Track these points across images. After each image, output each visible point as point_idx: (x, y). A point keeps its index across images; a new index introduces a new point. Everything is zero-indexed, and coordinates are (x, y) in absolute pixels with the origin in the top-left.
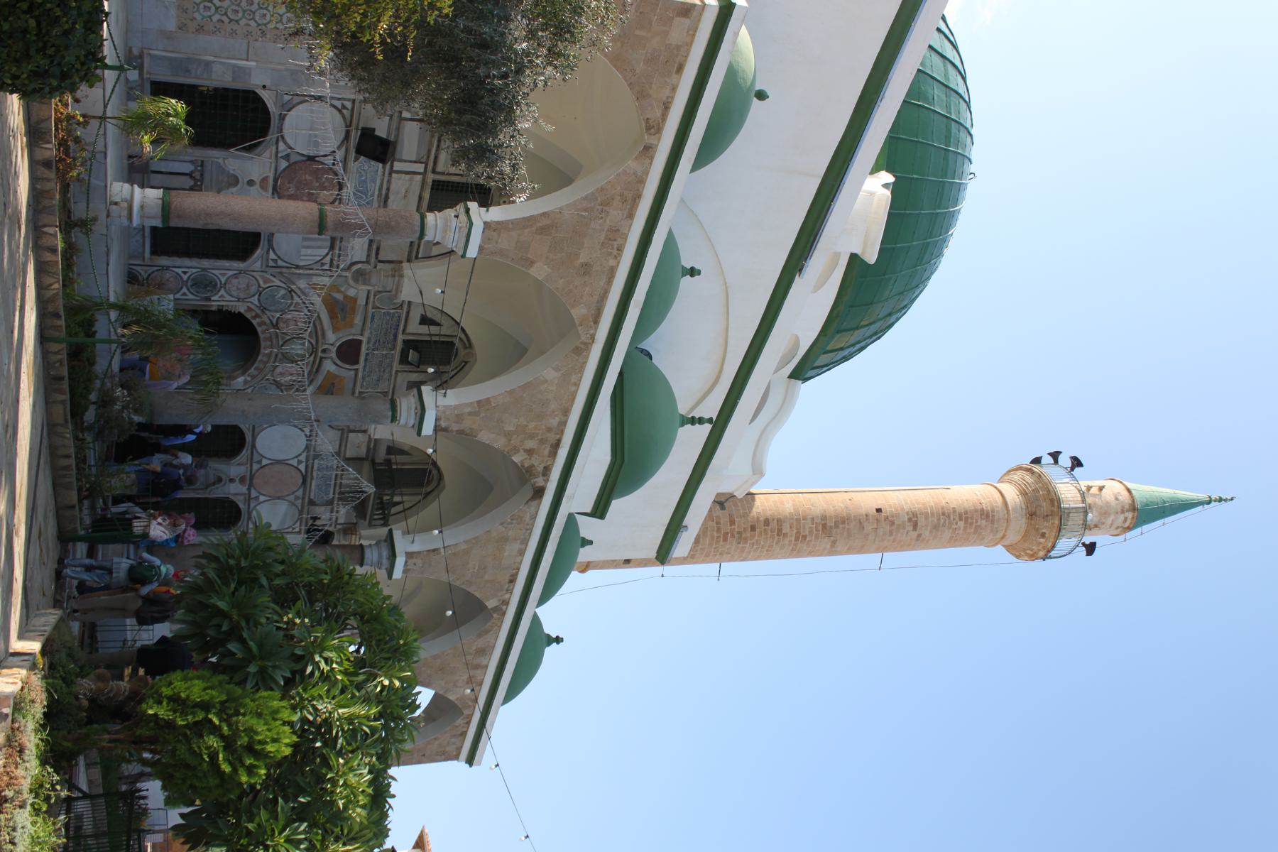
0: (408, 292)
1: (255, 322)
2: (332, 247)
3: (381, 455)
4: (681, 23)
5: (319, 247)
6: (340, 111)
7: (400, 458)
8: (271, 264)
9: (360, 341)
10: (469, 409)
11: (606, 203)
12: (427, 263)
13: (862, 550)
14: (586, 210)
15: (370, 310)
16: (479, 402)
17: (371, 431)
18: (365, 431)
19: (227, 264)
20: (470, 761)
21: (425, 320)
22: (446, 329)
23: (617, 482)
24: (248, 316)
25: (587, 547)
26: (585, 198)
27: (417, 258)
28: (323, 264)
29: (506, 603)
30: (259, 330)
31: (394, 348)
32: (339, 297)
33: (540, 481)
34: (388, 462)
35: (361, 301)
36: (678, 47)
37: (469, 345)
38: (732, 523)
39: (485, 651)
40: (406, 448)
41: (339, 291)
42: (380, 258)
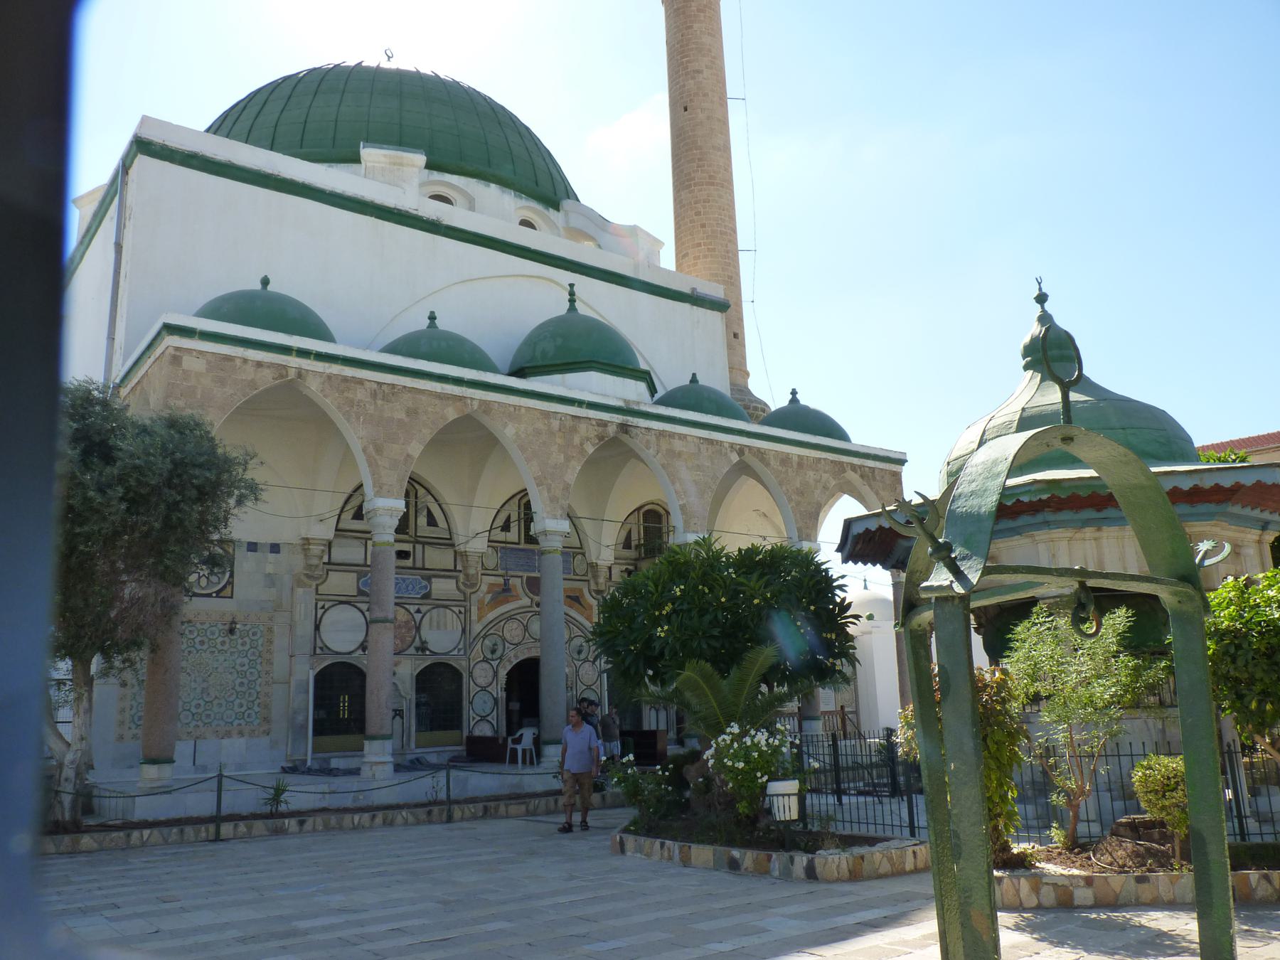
0: (479, 545)
2: (446, 607)
3: (632, 554)
4: (187, 362)
7: (634, 536)
9: (528, 578)
11: (351, 403)
13: (724, 122)
14: (358, 418)
16: (538, 485)
17: (608, 564)
18: (610, 568)
19: (465, 687)
20: (902, 462)
21: (506, 527)
24: (509, 668)
25: (698, 377)
26: (348, 420)
29: (732, 445)
30: (522, 658)
33: (611, 430)
34: (637, 547)
35: (492, 580)
36: (209, 362)
38: (699, 245)
39: (785, 460)
40: (624, 534)
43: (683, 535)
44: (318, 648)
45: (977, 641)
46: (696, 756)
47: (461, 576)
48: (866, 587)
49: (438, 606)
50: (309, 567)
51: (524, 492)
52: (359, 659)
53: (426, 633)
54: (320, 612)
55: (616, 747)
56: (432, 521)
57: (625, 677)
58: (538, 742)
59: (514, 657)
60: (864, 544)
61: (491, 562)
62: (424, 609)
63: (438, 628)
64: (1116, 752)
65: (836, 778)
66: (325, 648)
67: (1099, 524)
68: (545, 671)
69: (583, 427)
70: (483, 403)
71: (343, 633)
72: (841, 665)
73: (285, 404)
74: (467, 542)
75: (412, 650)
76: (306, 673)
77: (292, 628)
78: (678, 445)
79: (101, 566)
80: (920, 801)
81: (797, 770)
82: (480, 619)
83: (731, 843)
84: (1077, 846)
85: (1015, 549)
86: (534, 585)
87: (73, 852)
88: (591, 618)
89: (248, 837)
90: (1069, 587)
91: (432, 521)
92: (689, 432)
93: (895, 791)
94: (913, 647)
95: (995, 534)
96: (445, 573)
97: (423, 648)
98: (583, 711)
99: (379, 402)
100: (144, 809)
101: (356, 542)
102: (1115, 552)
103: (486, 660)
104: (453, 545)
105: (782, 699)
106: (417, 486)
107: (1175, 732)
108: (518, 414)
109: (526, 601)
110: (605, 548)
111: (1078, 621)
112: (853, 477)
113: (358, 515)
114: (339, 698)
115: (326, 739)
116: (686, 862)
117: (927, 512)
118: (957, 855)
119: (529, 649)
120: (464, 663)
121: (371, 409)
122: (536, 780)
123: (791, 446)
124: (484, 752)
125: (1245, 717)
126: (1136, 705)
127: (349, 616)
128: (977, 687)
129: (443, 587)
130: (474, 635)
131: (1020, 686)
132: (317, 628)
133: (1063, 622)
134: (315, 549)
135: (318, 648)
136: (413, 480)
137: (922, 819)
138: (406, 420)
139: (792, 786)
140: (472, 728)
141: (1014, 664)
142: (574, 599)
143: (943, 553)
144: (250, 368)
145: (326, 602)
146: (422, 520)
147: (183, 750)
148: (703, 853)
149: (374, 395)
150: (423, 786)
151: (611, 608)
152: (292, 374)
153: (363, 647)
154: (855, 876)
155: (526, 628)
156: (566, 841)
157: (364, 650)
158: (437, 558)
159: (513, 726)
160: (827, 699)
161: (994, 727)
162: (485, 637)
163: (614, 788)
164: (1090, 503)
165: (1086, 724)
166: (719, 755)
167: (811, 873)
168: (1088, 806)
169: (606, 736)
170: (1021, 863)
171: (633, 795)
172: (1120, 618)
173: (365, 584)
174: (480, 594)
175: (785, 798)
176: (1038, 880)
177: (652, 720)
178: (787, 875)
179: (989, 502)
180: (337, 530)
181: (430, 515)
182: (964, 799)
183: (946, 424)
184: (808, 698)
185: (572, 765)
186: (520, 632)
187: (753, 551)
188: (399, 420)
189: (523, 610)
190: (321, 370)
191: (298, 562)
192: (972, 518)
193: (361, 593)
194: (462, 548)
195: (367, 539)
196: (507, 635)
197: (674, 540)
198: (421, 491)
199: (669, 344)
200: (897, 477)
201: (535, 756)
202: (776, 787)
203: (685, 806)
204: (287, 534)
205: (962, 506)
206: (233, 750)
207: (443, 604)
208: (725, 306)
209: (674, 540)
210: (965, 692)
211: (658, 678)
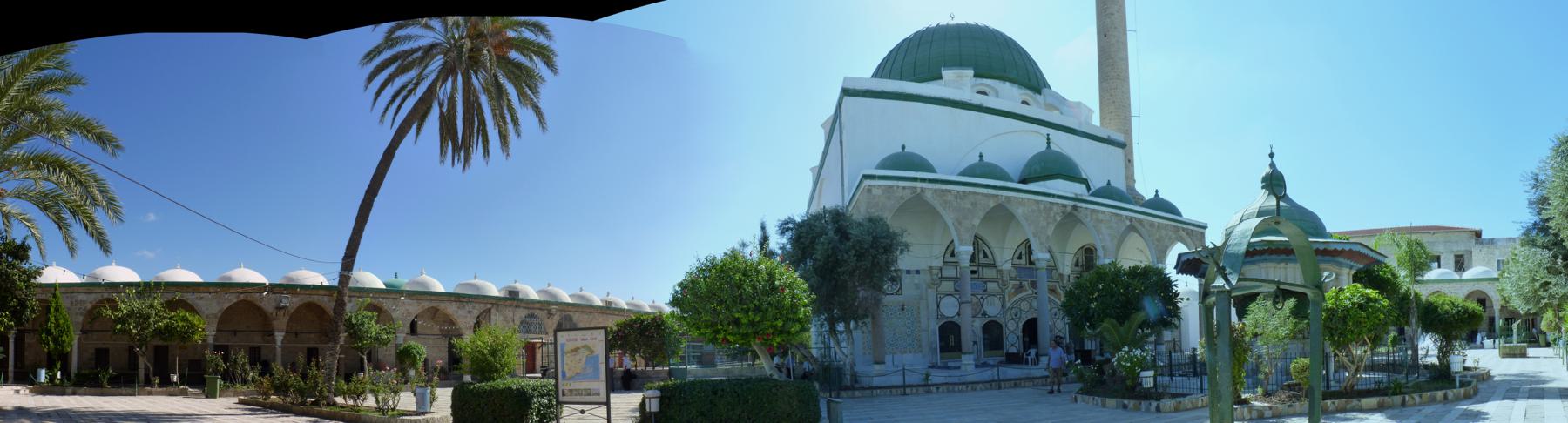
0: (1008, 266)
23: (1072, 175)
43: (1103, 260)
44: (939, 315)
45: (1233, 310)
46: (1108, 361)
48: (1186, 285)
51: (1028, 241)
52: (957, 320)
55: (1073, 357)
56: (986, 256)
57: (1076, 327)
58: (1037, 355)
59: (1025, 318)
60: (1186, 266)
64: (1286, 357)
65: (1170, 370)
67: (1286, 262)
68: (1040, 324)
71: (949, 308)
72: (1174, 320)
73: (917, 205)
76: (935, 326)
78: (1101, 216)
79: (850, 284)
80: (1206, 378)
81: (1154, 366)
83: (1124, 397)
84: (1267, 394)
85: (1253, 271)
86: (1034, 285)
87: (853, 397)
88: (1060, 299)
89: (917, 394)
90: (1272, 288)
91: (986, 256)
92: (1107, 209)
93: (1195, 374)
94: (1206, 312)
95: (1244, 263)
97: (985, 314)
98: (1058, 341)
100: (876, 382)
102: (1291, 274)
105: (1147, 336)
107: (1308, 349)
108: (1023, 202)
110: (1067, 266)
111: (1275, 303)
112: (1183, 234)
113: (953, 255)
114: (950, 337)
115: (946, 355)
116: (1104, 406)
117: (1216, 252)
118: (1219, 400)
122: (1037, 371)
123: (1154, 218)
124: (1013, 359)
125: (1333, 343)
126: (1294, 338)
127: (952, 300)
128: (1232, 330)
129: (992, 286)
131: (1250, 330)
133: (1269, 303)
135: (939, 315)
136: (976, 237)
137: (1206, 386)
139: (1151, 373)
140: (1008, 349)
141: (1248, 321)
142: (1053, 291)
143: (1221, 272)
147: (888, 358)
148: (1111, 402)
150: (988, 374)
151: (1069, 294)
154: (1177, 410)
156: (1051, 397)
159: (1026, 347)
160: (1167, 335)
161: (1238, 347)
163: (1072, 374)
164: (1282, 252)
165: (1275, 346)
166: (1119, 360)
167: (1158, 409)
168: (1273, 379)
169: (1068, 352)
170: (1245, 402)
171: (1081, 377)
172: (1291, 302)
175: (1148, 378)
176: (1251, 408)
177: (1088, 345)
178: (1148, 410)
179: (1243, 249)
182: (1224, 379)
183: (1225, 211)
184: (1159, 336)
185: (1053, 365)
187: (1136, 268)
189: (1029, 296)
191: (928, 277)
192: (1235, 255)
197: (1099, 262)
199: (1096, 164)
200: (1203, 235)
201: (1037, 361)
202: (1144, 374)
203: (1103, 382)
204: (922, 265)
205: (1231, 250)
206: (908, 358)
207: (993, 294)
208: (1124, 146)
209: (1099, 262)
210: (1227, 332)
211: (1092, 326)
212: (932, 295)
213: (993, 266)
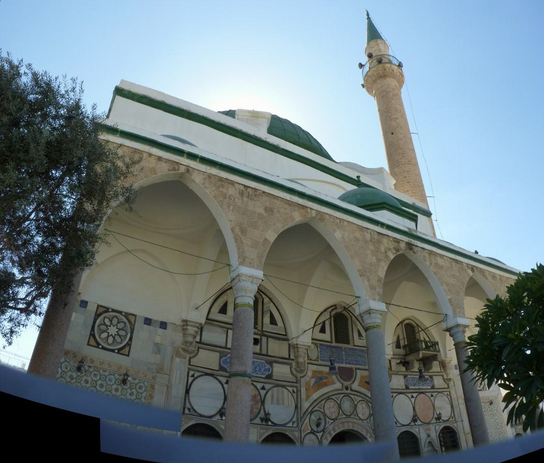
0: (305, 340)
1: (333, 434)
2: (283, 386)
5: (283, 393)
6: (196, 378)
8: (295, 425)
9: (339, 367)
10: (366, 283)
11: (225, 196)
12: (288, 330)
14: (229, 207)
15: (320, 362)
16: (361, 276)
21: (323, 330)
22: (327, 316)
26: (221, 208)
27: (286, 335)
28: (294, 392)
30: (338, 431)
31: (340, 348)
32: (313, 381)
35: (315, 368)
37: (335, 307)
41: (310, 381)
42: (287, 357)
44: (188, 409)
47: (294, 364)
49: (277, 386)
50: (187, 342)
53: (270, 407)
54: (191, 379)
56: (273, 321)
61: (314, 354)
62: (267, 386)
63: (278, 404)
66: (192, 409)
69: (385, 241)
70: (318, 212)
71: (206, 399)
74: (298, 337)
75: (258, 421)
77: (169, 387)
82: (308, 398)
91: (273, 321)
96: (283, 361)
97: (266, 419)
99: (245, 199)
101: (220, 330)
103: (313, 432)
104: (287, 340)
106: (264, 296)
109: (338, 385)
119: (343, 423)
120: (297, 434)
121: (239, 202)
129: (281, 371)
130: (304, 410)
132: (187, 391)
134: (191, 330)
136: (261, 291)
138: (265, 214)
144: (152, 159)
145: (195, 373)
146: (267, 320)
149: (242, 194)
152: (182, 169)
153: (221, 413)
155: (340, 407)
157: (221, 416)
158: (277, 348)
162: (312, 412)
173: (225, 362)
174: (307, 378)
180: (207, 319)
181: (272, 316)
186: (335, 409)
188: (260, 214)
190: (204, 170)
193: (221, 368)
194: (294, 341)
195: (228, 329)
196: (327, 412)
198: (266, 300)
212: (180, 367)
213: (283, 337)
